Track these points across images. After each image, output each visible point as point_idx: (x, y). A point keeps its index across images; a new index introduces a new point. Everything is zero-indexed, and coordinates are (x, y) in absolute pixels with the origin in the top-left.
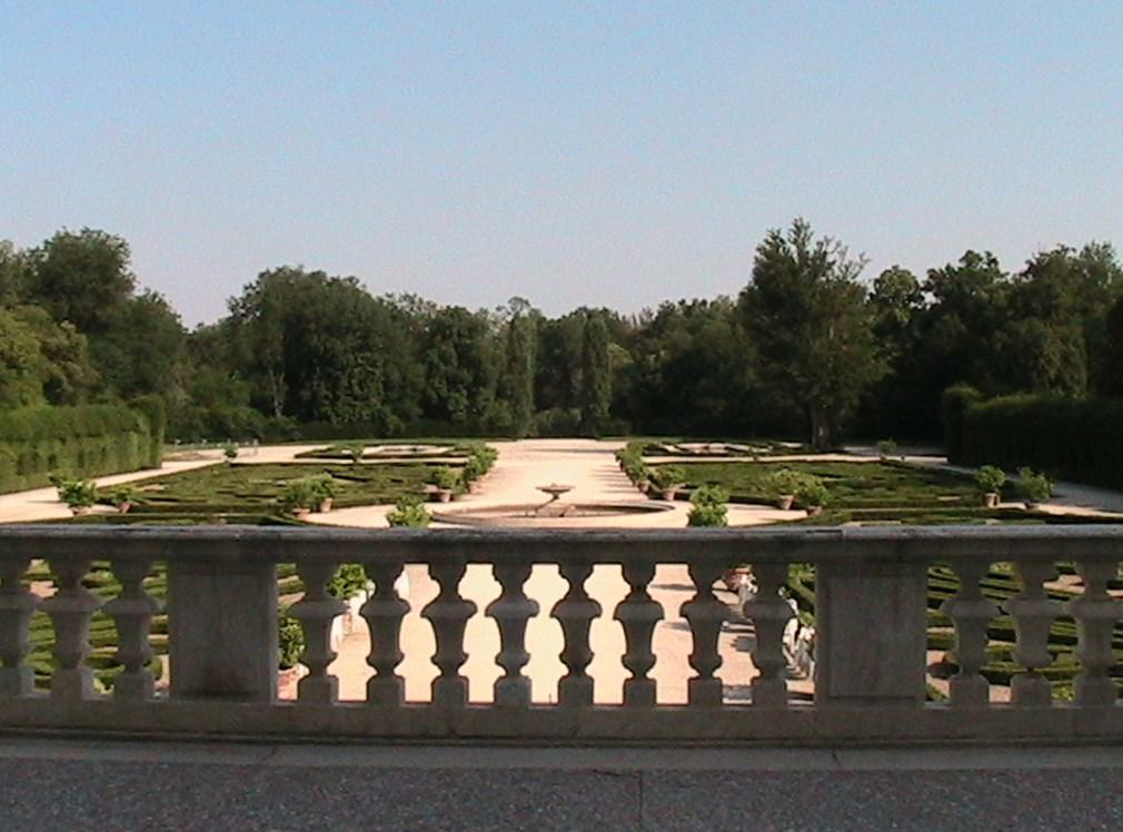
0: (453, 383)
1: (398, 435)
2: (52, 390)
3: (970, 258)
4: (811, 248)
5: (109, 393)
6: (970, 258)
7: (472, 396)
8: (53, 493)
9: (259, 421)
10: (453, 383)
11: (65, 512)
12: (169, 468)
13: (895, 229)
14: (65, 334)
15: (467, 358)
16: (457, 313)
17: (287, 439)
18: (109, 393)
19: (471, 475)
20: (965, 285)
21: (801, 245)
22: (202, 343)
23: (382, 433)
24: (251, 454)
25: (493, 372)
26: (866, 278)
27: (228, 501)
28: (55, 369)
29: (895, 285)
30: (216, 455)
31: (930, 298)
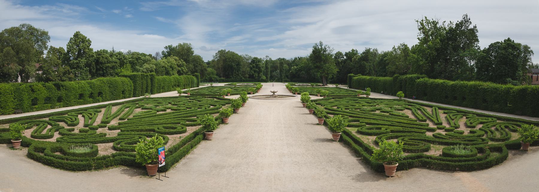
0: (255, 71)
1: (244, 81)
2: (179, 73)
3: (353, 50)
4: (323, 47)
5: (189, 73)
6: (353, 50)
7: (259, 74)
8: (176, 92)
9: (218, 78)
10: (255, 71)
11: (178, 95)
12: (200, 87)
13: (339, 45)
14: (182, 62)
15: (257, 66)
16: (256, 58)
17: (223, 81)
18: (189, 73)
19: (258, 90)
20: (351, 55)
21: (321, 46)
22: (208, 63)
23: (241, 81)
24: (215, 85)
25: (263, 69)
26: (334, 52)
27: (210, 93)
28: (180, 69)
29: (339, 54)
30: (209, 85)
31: (345, 57)
